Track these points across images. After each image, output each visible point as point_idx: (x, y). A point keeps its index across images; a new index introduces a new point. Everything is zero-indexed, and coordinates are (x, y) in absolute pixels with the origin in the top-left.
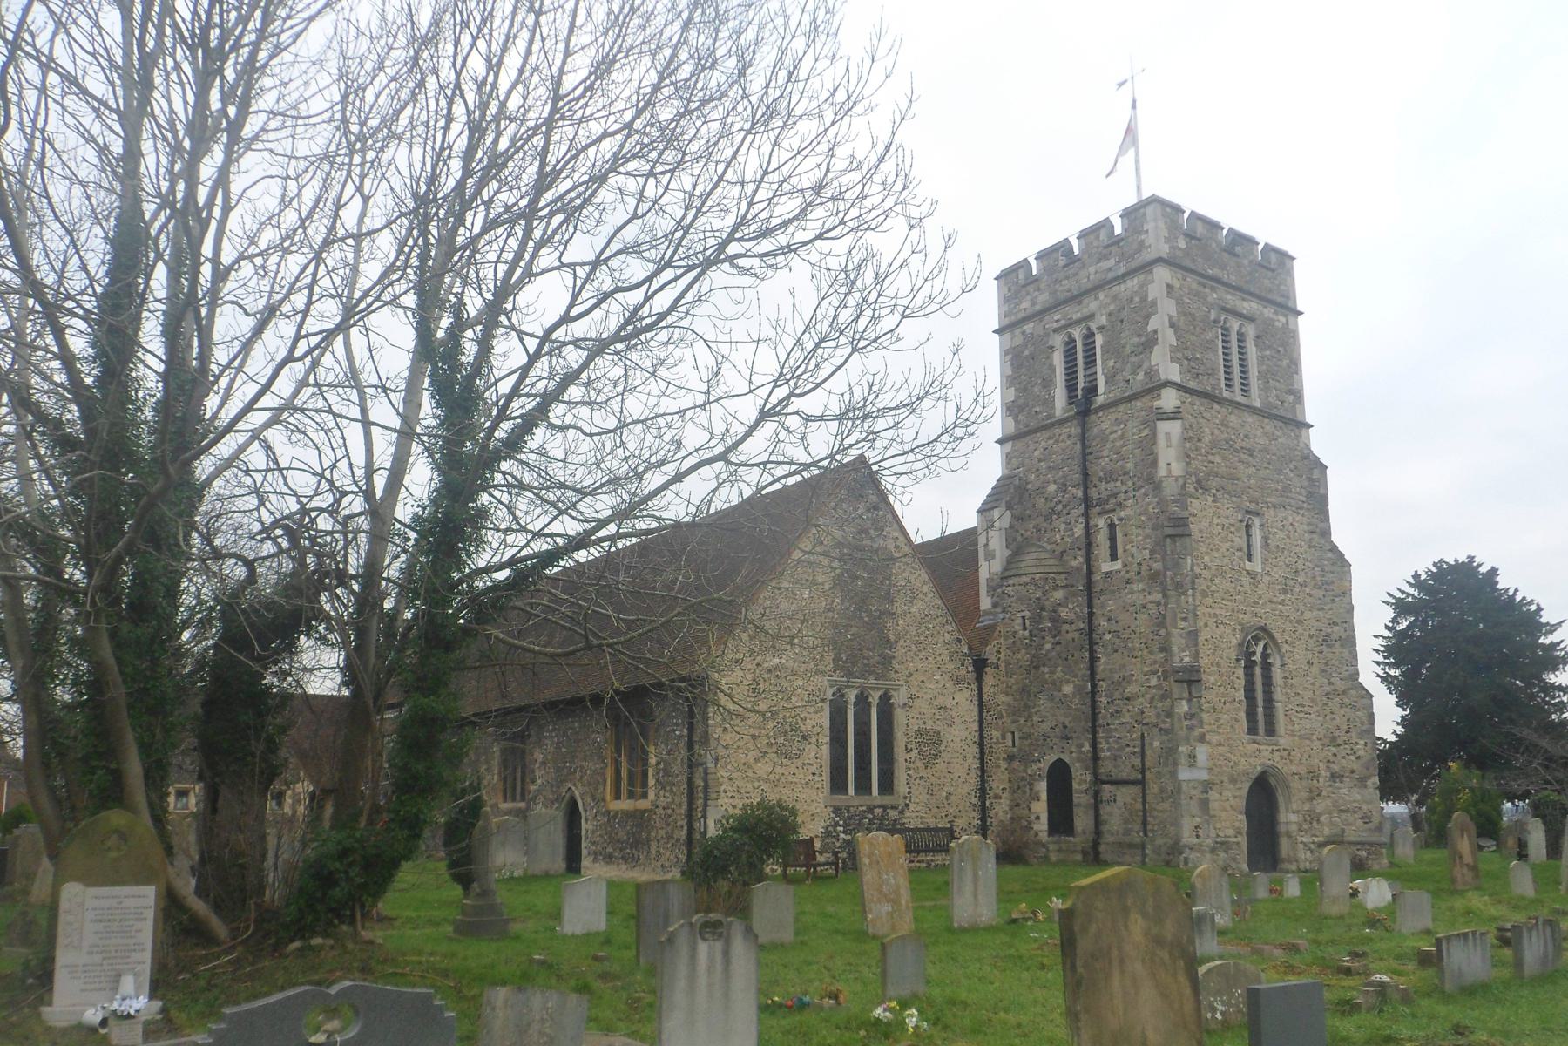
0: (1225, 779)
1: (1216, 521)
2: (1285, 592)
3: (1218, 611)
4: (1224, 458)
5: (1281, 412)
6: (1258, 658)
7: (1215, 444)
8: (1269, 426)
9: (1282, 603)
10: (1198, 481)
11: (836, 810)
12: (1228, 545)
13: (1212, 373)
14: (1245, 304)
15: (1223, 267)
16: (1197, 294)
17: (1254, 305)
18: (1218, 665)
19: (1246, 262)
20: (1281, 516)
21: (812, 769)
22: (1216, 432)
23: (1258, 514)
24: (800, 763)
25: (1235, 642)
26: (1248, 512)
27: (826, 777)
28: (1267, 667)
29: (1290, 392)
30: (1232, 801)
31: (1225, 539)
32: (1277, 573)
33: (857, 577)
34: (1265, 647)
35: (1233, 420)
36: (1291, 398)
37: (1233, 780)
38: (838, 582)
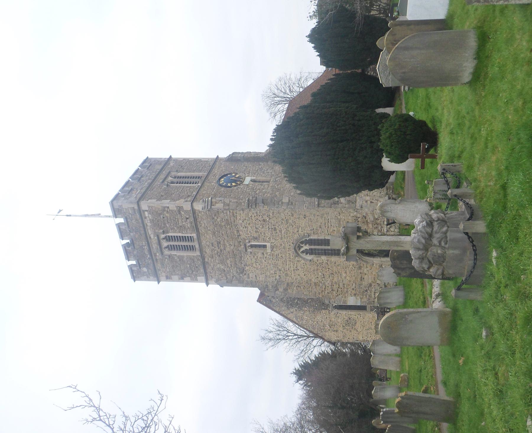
0: (359, 271)
1: (254, 265)
2: (275, 229)
3: (292, 269)
4: (227, 259)
5: (192, 219)
6: (307, 247)
7: (222, 262)
8: (202, 230)
9: (281, 231)
10: (242, 273)
11: (372, 310)
12: (263, 261)
13: (192, 259)
14: (152, 236)
15: (142, 247)
16: (162, 264)
17: (150, 233)
18: (314, 271)
19: (132, 234)
20: (242, 228)
21: (359, 317)
22: (217, 261)
23: (245, 245)
24: (357, 320)
25: (303, 261)
26: (246, 251)
27: (362, 313)
28: (311, 242)
29: (180, 213)
30: (368, 269)
31: (261, 262)
32: (268, 234)
33: (297, 302)
34: (302, 243)
35: (208, 251)
36: (183, 213)
37: (360, 268)
38: (300, 308)
